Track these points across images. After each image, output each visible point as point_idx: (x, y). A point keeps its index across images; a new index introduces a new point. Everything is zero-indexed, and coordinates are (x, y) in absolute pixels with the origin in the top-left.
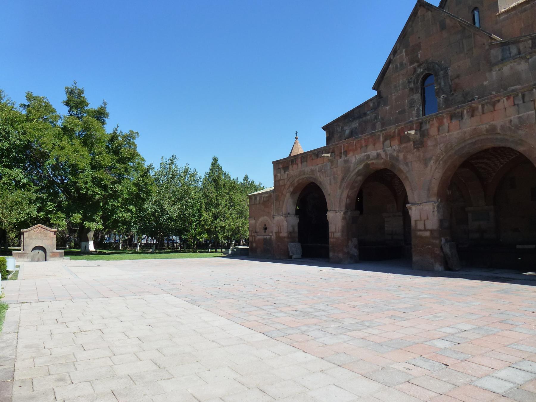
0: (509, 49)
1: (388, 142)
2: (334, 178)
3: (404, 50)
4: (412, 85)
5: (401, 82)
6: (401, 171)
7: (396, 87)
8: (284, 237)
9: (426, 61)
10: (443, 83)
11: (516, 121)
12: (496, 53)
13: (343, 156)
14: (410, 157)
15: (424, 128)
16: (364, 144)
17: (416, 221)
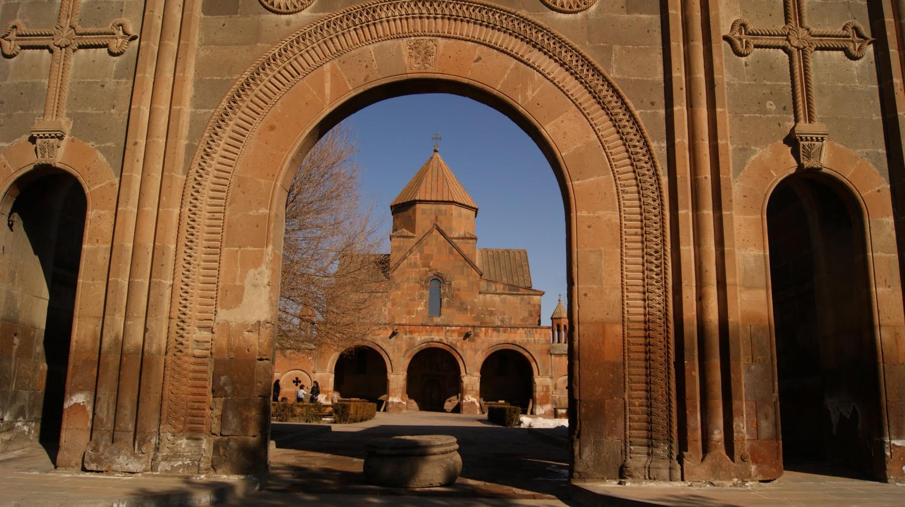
0: (491, 286)
1: (449, 333)
2: (398, 348)
3: (418, 254)
4: (423, 283)
5: (413, 277)
6: (458, 354)
7: (408, 279)
8: (330, 391)
9: (436, 269)
10: (447, 290)
11: (525, 341)
12: (483, 284)
13: (408, 334)
14: (465, 346)
15: (476, 331)
16: (429, 330)
17: (467, 385)
